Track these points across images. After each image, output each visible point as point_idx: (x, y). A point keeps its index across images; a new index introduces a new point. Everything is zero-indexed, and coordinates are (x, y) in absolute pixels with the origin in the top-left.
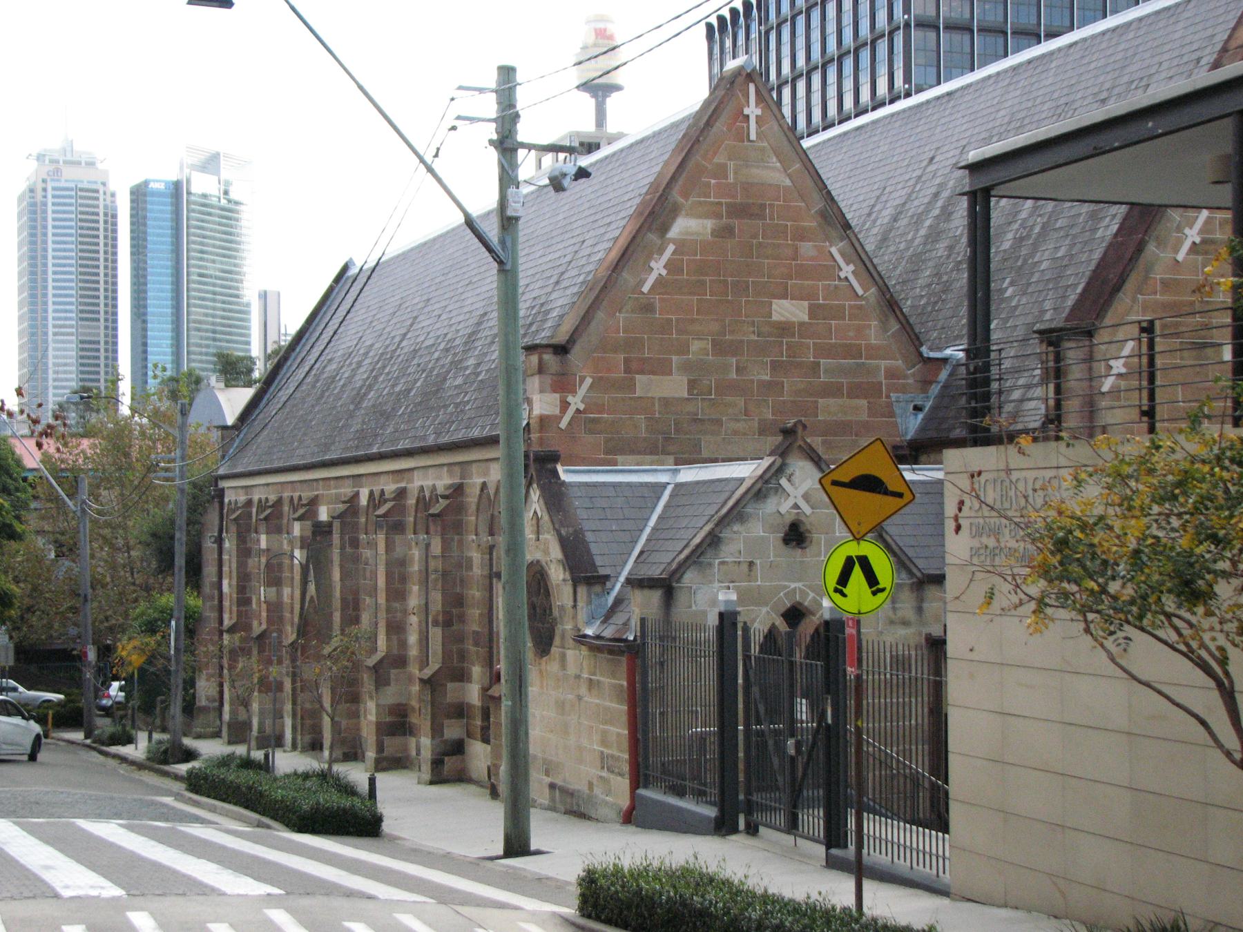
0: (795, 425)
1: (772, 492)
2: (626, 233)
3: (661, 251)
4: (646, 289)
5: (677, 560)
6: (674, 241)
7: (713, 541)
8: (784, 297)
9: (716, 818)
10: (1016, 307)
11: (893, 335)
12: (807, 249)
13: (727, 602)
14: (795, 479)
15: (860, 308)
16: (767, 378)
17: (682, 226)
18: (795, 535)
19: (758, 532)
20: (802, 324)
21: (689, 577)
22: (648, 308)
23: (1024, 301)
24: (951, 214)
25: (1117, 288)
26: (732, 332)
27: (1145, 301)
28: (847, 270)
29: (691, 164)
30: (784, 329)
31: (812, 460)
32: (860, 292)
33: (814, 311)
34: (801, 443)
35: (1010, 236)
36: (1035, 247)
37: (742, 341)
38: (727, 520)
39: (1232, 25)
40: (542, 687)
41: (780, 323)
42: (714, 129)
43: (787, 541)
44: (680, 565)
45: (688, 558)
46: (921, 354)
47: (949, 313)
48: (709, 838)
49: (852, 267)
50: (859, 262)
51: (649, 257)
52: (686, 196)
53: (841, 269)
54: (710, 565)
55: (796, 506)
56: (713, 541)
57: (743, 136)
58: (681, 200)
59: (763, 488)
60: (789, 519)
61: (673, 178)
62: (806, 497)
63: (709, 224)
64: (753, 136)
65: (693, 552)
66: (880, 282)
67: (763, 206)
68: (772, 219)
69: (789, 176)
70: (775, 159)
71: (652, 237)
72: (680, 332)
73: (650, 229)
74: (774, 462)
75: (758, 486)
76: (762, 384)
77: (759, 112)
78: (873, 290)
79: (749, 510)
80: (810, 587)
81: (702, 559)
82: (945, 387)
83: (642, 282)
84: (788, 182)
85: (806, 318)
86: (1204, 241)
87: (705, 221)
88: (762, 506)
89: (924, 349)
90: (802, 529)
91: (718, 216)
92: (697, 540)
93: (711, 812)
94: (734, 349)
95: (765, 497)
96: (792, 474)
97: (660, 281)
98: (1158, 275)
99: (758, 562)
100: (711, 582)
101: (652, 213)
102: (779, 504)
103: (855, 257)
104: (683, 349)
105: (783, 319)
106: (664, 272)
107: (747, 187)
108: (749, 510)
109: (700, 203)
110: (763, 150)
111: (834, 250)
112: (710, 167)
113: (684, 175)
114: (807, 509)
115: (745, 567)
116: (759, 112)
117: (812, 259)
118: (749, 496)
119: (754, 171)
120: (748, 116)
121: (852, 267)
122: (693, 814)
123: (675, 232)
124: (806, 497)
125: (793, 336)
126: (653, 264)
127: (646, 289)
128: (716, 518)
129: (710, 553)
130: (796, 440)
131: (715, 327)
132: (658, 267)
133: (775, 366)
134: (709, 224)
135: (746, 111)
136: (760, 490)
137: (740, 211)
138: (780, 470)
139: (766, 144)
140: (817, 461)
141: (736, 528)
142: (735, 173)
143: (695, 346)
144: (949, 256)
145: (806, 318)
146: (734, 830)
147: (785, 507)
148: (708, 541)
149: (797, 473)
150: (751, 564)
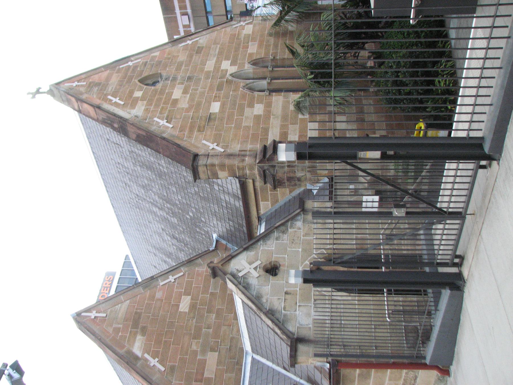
0: (209, 267)
1: (246, 280)
2: (135, 376)
3: (146, 360)
4: (163, 369)
5: (281, 336)
6: (143, 354)
7: (271, 314)
8: (178, 306)
9: (451, 289)
10: (196, 209)
11: (203, 262)
12: (159, 295)
13: (296, 276)
14: (239, 268)
15: (189, 274)
16: (214, 315)
17: (137, 349)
18: (272, 270)
19: (268, 290)
20: (192, 299)
21: (292, 328)
22: (172, 369)
23: (193, 205)
24: (170, 253)
25: (178, 146)
26: (190, 330)
27: (187, 137)
28: (171, 278)
29: (110, 343)
30: (193, 307)
31: (230, 259)
32: (182, 274)
33: (187, 294)
34: (220, 265)
35: (172, 219)
36: (174, 205)
37: (195, 326)
38: (260, 305)
39: (91, 120)
40: (309, 167)
41: (190, 308)
42: (97, 332)
43: (275, 275)
44: (284, 332)
45: (280, 329)
46: (213, 251)
47: (202, 246)
48: (466, 295)
49: (171, 277)
50: (168, 274)
51: (148, 366)
52: (123, 347)
53: (170, 281)
54: (285, 315)
55: (255, 269)
56: (271, 314)
57: (103, 319)
58: (125, 349)
59: (244, 286)
60: (263, 273)
61: (114, 352)
62: (250, 263)
63: (139, 337)
64: (104, 315)
65: (276, 325)
66: (179, 265)
67: (136, 313)
68: (142, 309)
69: (125, 301)
70: (117, 306)
71: (139, 364)
72: (186, 354)
73: (135, 365)
74: (228, 278)
75: (241, 287)
76: (217, 318)
77: (94, 312)
78: (182, 269)
79: (254, 293)
80: (302, 263)
81: (281, 320)
82: (228, 241)
83: (159, 370)
84: (128, 302)
85: (189, 297)
86: (166, 119)
87: (137, 339)
88: (253, 286)
89: (211, 249)
90: (269, 266)
91: (135, 334)
92: (269, 323)
93: (446, 294)
94: (198, 329)
95: (248, 284)
96: (237, 270)
97: (161, 362)
98: (176, 133)
99: (285, 289)
100: (295, 315)
101: (127, 363)
102: (253, 277)
103: (166, 275)
104: (195, 353)
105: (188, 307)
106: (157, 359)
107: (126, 320)
108: (254, 293)
109: (128, 341)
110: (111, 311)
111: (161, 284)
112: (113, 335)
113: (115, 347)
114: (258, 263)
115: (288, 296)
116: (94, 312)
117: (163, 293)
118: (246, 292)
119: (120, 315)
120: (95, 317)
121: (171, 277)
122: (446, 312)
123: (139, 353)
124: (250, 263)
125: (197, 303)
126: (152, 365)
127: (163, 369)
128: (258, 312)
129: (277, 315)
130: (218, 267)
131: (187, 338)
132: (154, 362)
133: (209, 311)
134: (139, 337)
135: (93, 317)
136: (244, 287)
137: (136, 324)
138: (234, 276)
139: (109, 310)
140: (232, 257)
141: (264, 300)
142: (119, 324)
143: (194, 347)
144: (183, 251)
145: (189, 297)
146: (459, 276)
147: (255, 274)
148: (270, 316)
149: (237, 267)
150: (286, 293)
